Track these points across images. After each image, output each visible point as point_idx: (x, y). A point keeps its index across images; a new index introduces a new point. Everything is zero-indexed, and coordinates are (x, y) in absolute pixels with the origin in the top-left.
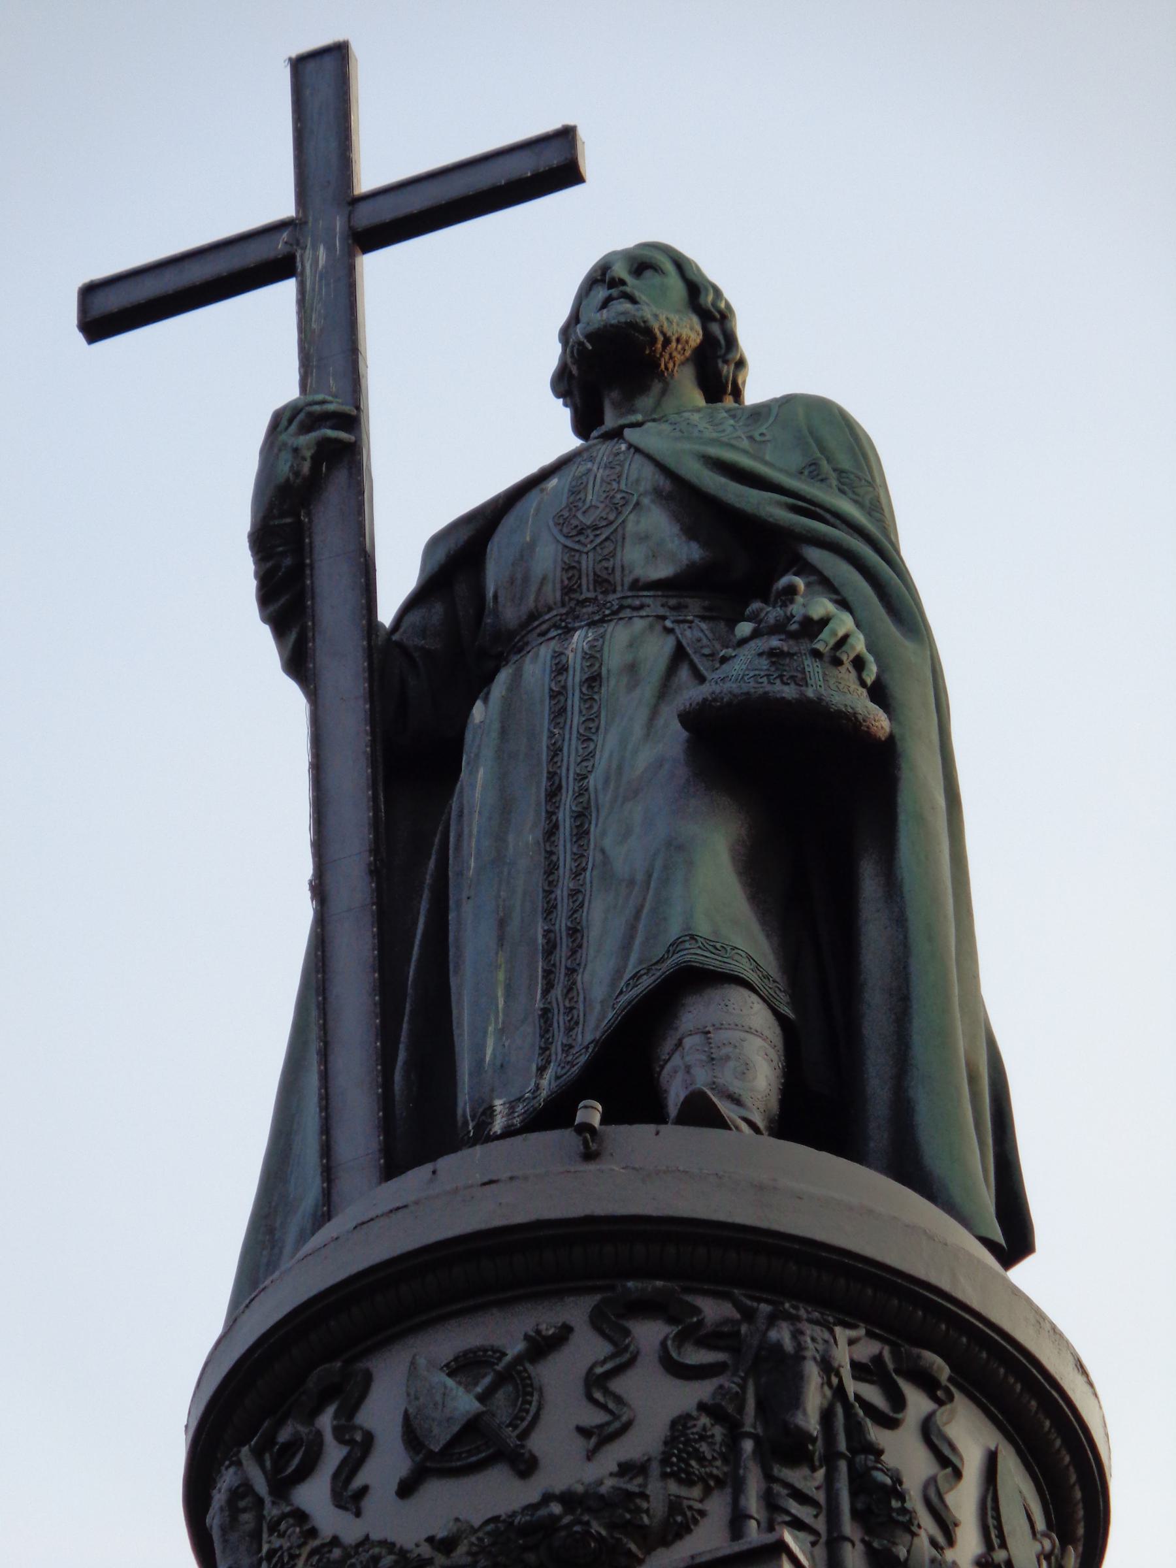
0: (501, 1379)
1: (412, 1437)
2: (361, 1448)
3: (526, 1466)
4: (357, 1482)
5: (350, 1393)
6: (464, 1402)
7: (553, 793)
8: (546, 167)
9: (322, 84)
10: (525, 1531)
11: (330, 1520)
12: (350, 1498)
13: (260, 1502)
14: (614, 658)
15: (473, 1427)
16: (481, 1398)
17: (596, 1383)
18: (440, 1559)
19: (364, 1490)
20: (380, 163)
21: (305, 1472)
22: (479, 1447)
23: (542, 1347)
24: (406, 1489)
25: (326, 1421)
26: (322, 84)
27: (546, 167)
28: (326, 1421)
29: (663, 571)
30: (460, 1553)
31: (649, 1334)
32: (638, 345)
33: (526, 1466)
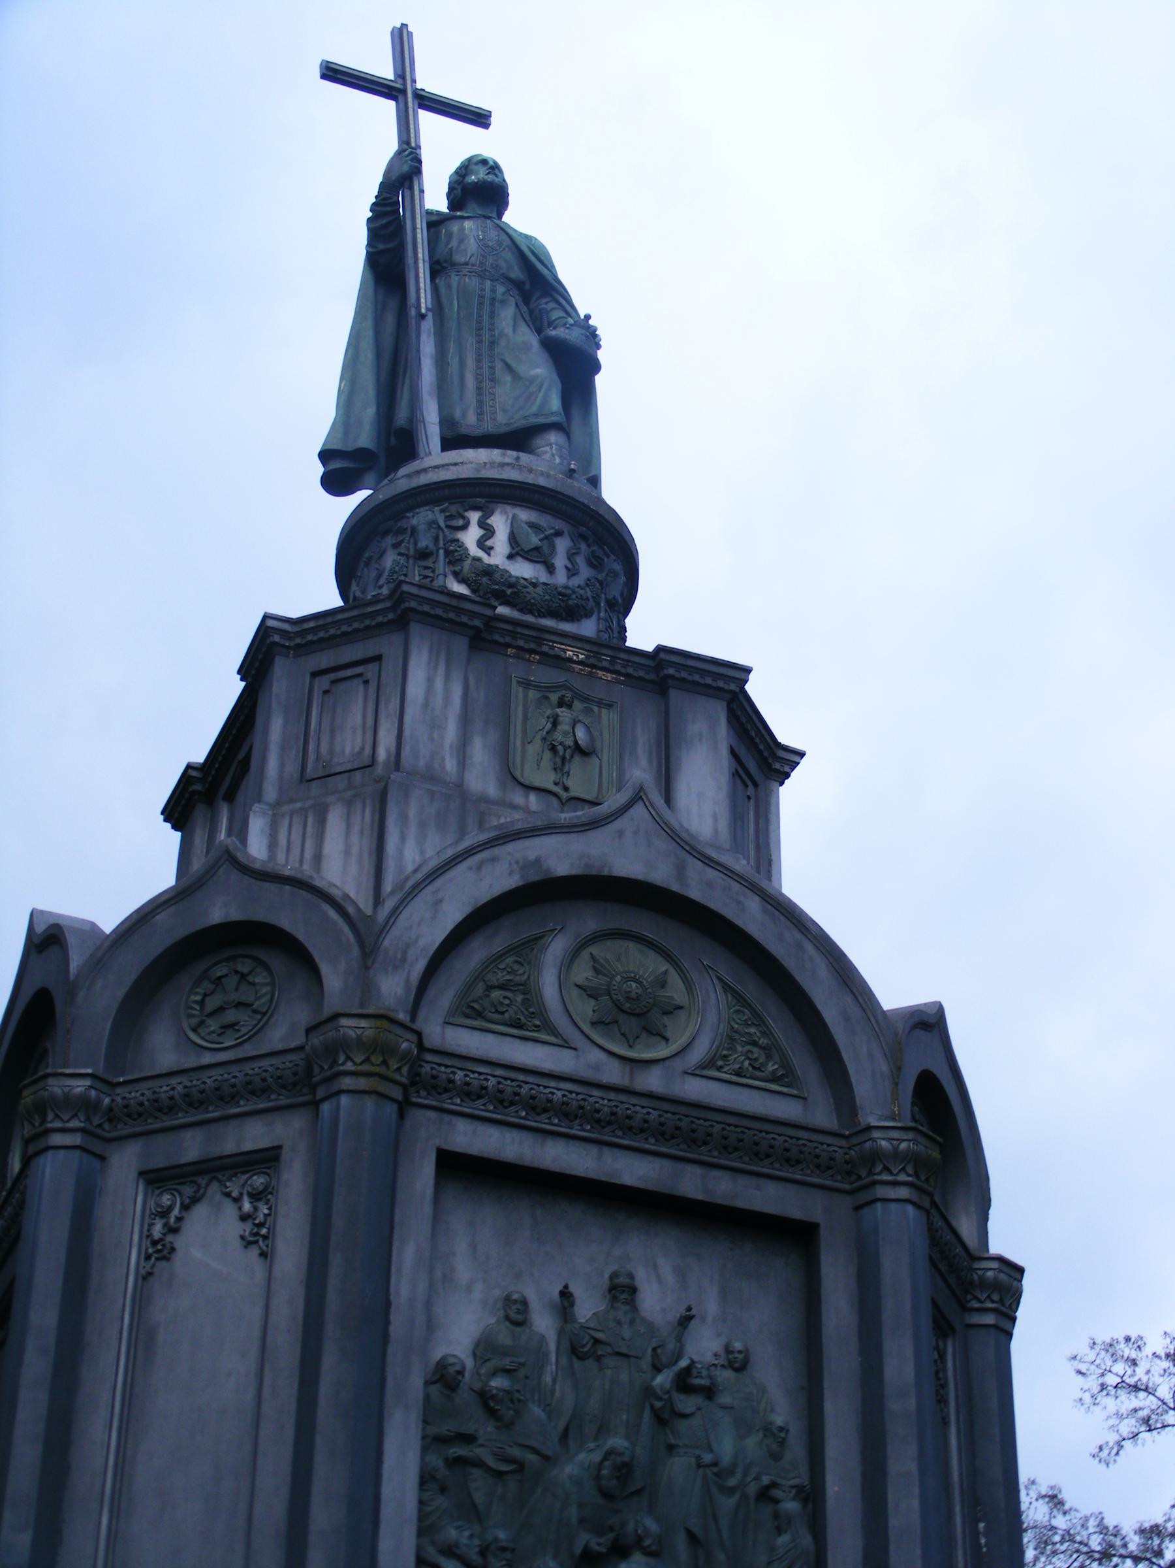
0: (546, 538)
1: (513, 539)
2: (489, 532)
3: (551, 569)
4: (488, 543)
5: (487, 513)
6: (535, 540)
7: (479, 329)
8: (479, 118)
9: (401, 39)
10: (560, 594)
11: (474, 550)
12: (481, 544)
13: (439, 527)
14: (499, 296)
15: (537, 549)
16: (541, 540)
17: (571, 556)
18: (531, 589)
19: (491, 548)
20: (427, 80)
21: (465, 527)
22: (539, 556)
23: (558, 534)
24: (510, 557)
25: (474, 516)
26: (401, 39)
27: (479, 118)
28: (474, 516)
29: (512, 275)
30: (539, 590)
31: (583, 546)
32: (480, 189)
33: (551, 569)
